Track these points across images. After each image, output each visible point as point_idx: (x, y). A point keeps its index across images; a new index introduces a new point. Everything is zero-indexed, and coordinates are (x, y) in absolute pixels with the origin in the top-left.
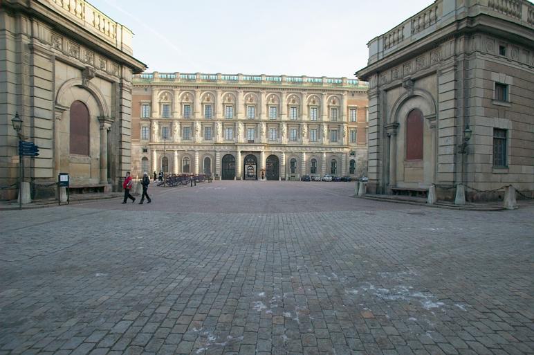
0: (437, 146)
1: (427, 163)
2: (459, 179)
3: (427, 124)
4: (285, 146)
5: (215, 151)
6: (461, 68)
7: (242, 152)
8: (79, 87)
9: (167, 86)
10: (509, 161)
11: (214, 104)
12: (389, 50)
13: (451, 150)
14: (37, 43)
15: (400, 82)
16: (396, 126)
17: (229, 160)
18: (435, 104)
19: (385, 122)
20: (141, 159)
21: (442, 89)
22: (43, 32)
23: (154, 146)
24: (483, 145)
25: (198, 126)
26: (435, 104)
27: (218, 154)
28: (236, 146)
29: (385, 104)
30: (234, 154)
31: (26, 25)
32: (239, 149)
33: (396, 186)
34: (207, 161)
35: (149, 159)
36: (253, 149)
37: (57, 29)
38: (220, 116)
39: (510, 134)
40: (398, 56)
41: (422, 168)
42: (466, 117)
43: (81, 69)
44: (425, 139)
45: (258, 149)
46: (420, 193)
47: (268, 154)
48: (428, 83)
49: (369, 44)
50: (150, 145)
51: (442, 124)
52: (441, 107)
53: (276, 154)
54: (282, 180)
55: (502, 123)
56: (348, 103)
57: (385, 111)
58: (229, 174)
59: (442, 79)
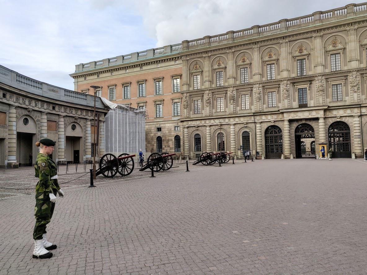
4: (360, 106)
5: (255, 122)
7: (291, 121)
9: (196, 54)
11: (251, 64)
17: (273, 134)
20: (174, 138)
23: (185, 123)
27: (258, 125)
28: (282, 113)
30: (279, 124)
34: (246, 137)
35: (181, 137)
45: (314, 115)
50: (182, 121)
53: (343, 120)
54: (356, 157)
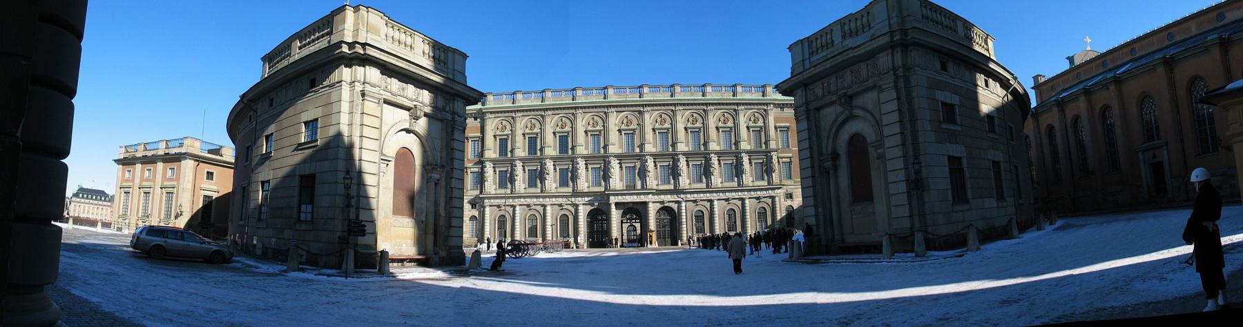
0: (887, 183)
1: (880, 208)
2: (917, 225)
3: (873, 153)
6: (901, 84)
7: (617, 204)
8: (408, 131)
10: (970, 195)
12: (818, 57)
13: (903, 187)
14: (368, 88)
15: (834, 98)
16: (835, 156)
18: (879, 125)
19: (820, 153)
21: (885, 108)
22: (373, 73)
24: (939, 178)
25: (550, 165)
26: (879, 125)
29: (818, 127)
30: (604, 209)
31: (360, 70)
32: (613, 200)
33: (843, 241)
36: (634, 199)
37: (388, 70)
38: (581, 150)
39: (964, 161)
40: (828, 65)
41: (874, 213)
42: (916, 145)
43: (408, 109)
44: (873, 173)
45: (643, 198)
46: (875, 247)
47: (659, 206)
48: (868, 99)
49: (790, 48)
51: (890, 154)
52: (886, 131)
55: (957, 150)
56: (776, 120)
57: (819, 137)
58: (599, 237)
59: (885, 96)
